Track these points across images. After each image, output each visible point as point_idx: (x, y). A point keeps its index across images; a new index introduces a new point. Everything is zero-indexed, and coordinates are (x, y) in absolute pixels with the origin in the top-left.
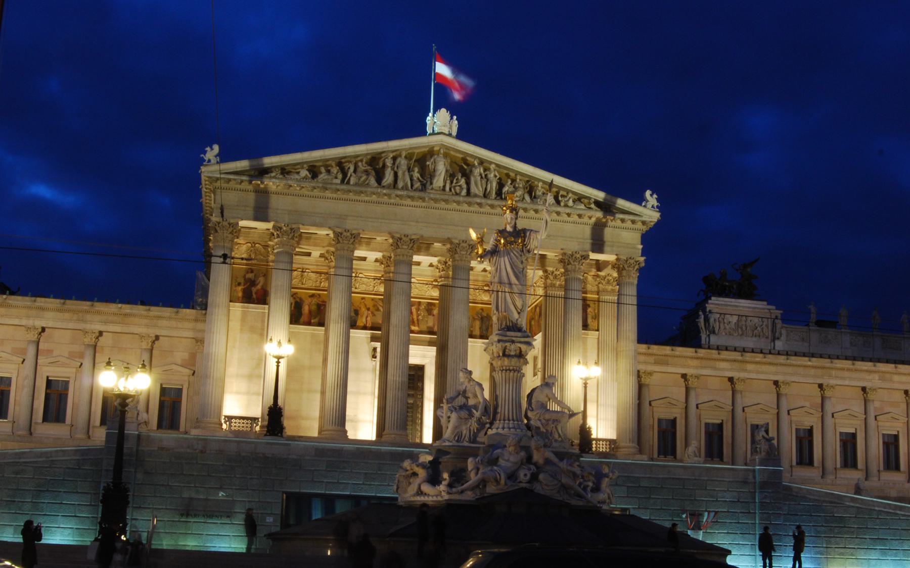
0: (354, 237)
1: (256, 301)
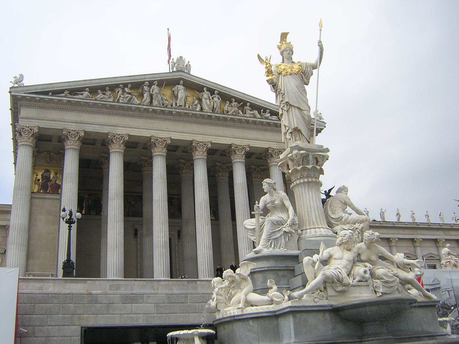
0: (124, 139)
1: (51, 192)
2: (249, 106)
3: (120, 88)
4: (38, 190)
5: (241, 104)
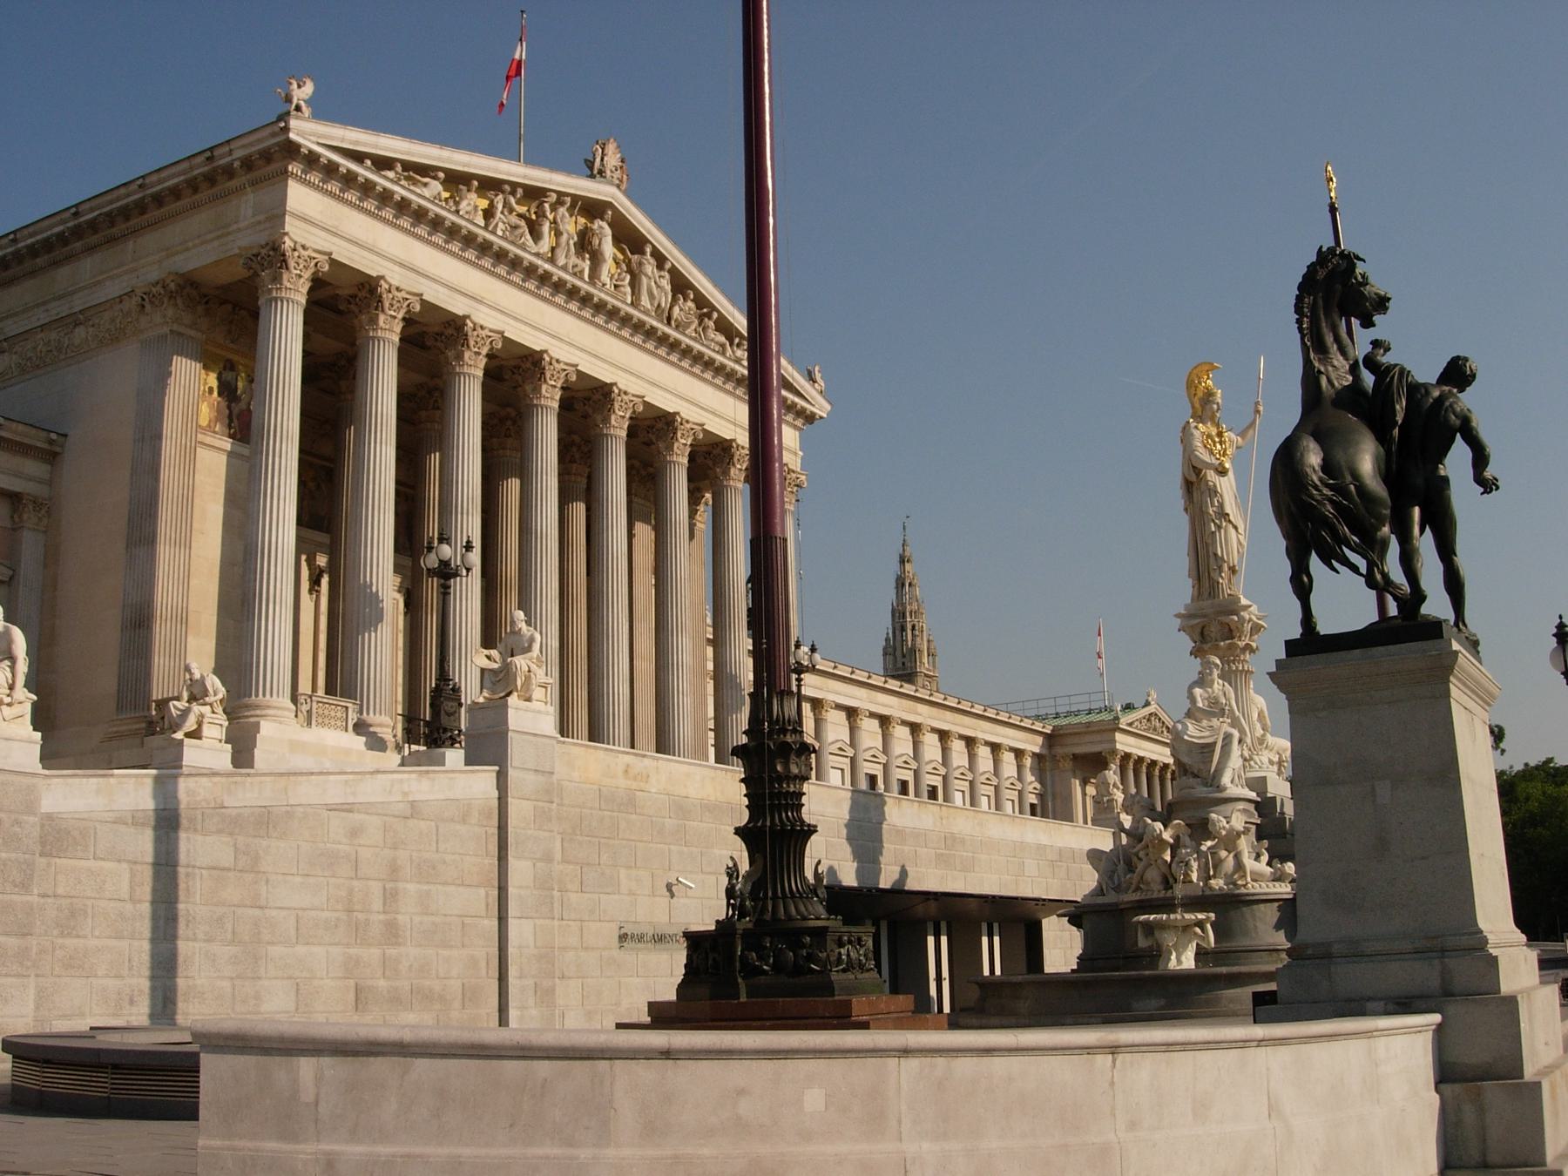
2: (714, 323)
3: (503, 192)
4: (210, 421)
5: (705, 310)
